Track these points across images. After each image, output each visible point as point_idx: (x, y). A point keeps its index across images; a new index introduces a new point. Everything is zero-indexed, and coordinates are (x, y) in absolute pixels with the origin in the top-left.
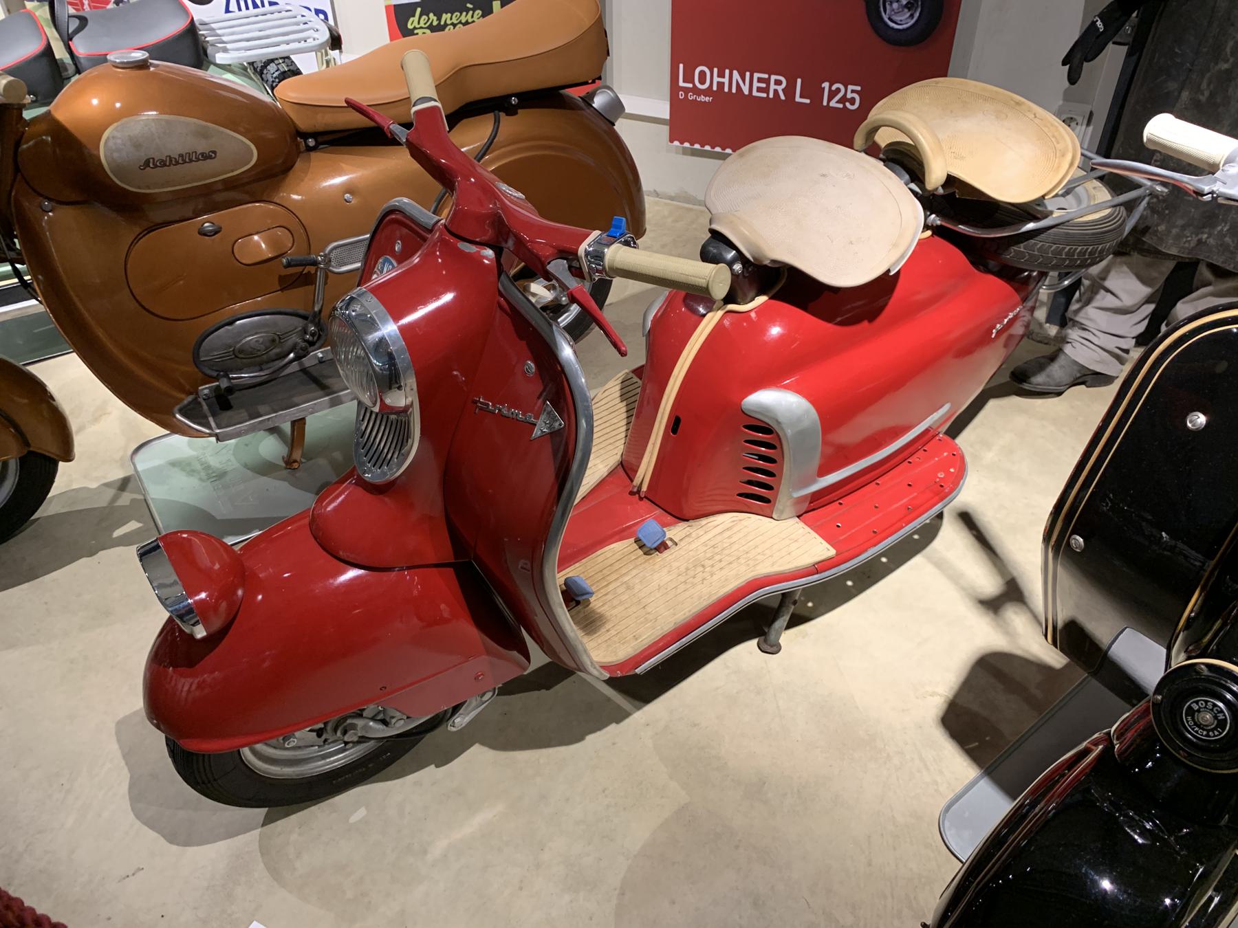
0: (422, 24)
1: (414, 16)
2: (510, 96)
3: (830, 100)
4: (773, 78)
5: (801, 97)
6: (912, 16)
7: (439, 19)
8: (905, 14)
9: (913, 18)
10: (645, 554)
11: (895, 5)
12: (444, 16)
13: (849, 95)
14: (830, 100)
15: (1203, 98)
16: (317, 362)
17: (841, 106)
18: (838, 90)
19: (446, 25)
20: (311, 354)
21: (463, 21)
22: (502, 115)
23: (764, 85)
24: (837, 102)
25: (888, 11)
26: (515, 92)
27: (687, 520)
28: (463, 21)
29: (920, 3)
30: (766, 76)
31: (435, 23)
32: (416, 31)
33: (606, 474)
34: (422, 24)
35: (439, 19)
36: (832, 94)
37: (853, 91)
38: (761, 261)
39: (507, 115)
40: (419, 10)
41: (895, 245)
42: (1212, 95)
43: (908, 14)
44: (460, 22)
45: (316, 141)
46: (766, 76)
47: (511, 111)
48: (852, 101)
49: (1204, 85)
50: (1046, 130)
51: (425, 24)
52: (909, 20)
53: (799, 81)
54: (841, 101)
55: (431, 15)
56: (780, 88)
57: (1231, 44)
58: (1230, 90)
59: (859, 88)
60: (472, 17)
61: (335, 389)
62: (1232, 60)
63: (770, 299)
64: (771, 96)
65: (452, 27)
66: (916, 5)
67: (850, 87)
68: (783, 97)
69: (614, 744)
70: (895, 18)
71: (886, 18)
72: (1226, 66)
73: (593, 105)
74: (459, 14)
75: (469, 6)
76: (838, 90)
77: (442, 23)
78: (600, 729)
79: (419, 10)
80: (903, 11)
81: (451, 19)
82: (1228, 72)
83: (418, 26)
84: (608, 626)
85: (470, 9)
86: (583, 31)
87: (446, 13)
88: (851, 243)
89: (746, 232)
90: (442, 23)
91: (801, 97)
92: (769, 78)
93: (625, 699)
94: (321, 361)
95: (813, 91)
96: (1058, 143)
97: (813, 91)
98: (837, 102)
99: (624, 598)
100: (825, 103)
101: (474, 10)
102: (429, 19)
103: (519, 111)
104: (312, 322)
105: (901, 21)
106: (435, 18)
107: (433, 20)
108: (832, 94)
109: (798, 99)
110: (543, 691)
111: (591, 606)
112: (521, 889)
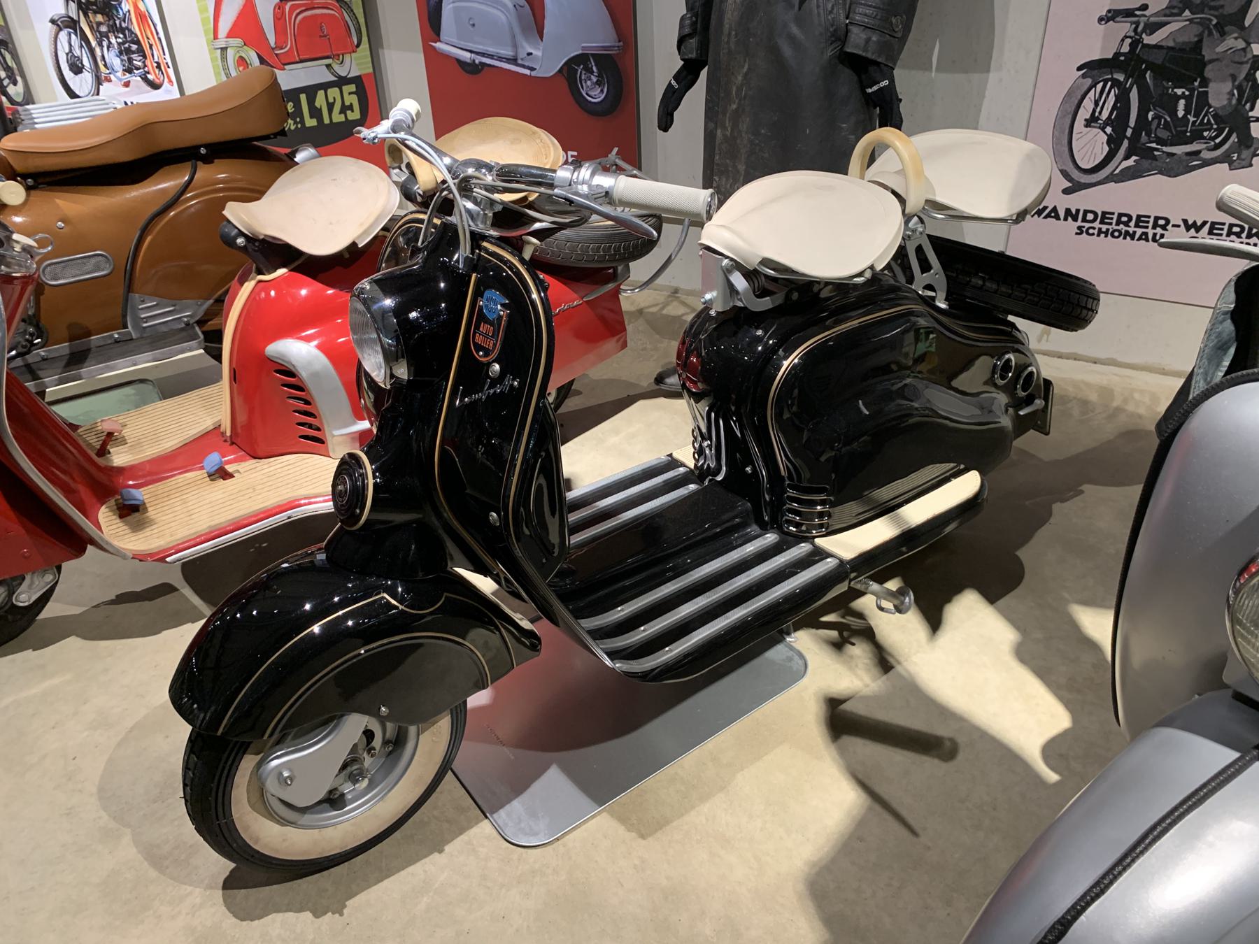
2: (201, 146)
6: (602, 91)
8: (597, 90)
9: (603, 93)
10: (211, 480)
11: (589, 83)
15: (728, 133)
16: (41, 359)
20: (34, 352)
22: (199, 163)
25: (584, 88)
26: (204, 142)
27: (261, 459)
29: (606, 80)
33: (212, 428)
38: (257, 237)
39: (204, 163)
41: (361, 224)
42: (732, 130)
43: (599, 90)
45: (35, 181)
47: (207, 160)
49: (727, 125)
50: (543, 150)
52: (600, 95)
57: (734, 89)
58: (740, 126)
59: (575, 153)
61: (42, 376)
62: (737, 101)
63: (290, 271)
66: (603, 82)
69: (182, 636)
70: (590, 93)
72: (734, 106)
73: (295, 159)
78: (176, 626)
80: (595, 87)
82: (737, 110)
84: (153, 527)
86: (255, 94)
88: (331, 224)
89: (244, 217)
93: (209, 607)
94: (44, 359)
96: (546, 158)
99: (176, 509)
103: (216, 161)
104: (30, 324)
105: (595, 95)
110: (147, 602)
111: (148, 514)
112: (53, 728)
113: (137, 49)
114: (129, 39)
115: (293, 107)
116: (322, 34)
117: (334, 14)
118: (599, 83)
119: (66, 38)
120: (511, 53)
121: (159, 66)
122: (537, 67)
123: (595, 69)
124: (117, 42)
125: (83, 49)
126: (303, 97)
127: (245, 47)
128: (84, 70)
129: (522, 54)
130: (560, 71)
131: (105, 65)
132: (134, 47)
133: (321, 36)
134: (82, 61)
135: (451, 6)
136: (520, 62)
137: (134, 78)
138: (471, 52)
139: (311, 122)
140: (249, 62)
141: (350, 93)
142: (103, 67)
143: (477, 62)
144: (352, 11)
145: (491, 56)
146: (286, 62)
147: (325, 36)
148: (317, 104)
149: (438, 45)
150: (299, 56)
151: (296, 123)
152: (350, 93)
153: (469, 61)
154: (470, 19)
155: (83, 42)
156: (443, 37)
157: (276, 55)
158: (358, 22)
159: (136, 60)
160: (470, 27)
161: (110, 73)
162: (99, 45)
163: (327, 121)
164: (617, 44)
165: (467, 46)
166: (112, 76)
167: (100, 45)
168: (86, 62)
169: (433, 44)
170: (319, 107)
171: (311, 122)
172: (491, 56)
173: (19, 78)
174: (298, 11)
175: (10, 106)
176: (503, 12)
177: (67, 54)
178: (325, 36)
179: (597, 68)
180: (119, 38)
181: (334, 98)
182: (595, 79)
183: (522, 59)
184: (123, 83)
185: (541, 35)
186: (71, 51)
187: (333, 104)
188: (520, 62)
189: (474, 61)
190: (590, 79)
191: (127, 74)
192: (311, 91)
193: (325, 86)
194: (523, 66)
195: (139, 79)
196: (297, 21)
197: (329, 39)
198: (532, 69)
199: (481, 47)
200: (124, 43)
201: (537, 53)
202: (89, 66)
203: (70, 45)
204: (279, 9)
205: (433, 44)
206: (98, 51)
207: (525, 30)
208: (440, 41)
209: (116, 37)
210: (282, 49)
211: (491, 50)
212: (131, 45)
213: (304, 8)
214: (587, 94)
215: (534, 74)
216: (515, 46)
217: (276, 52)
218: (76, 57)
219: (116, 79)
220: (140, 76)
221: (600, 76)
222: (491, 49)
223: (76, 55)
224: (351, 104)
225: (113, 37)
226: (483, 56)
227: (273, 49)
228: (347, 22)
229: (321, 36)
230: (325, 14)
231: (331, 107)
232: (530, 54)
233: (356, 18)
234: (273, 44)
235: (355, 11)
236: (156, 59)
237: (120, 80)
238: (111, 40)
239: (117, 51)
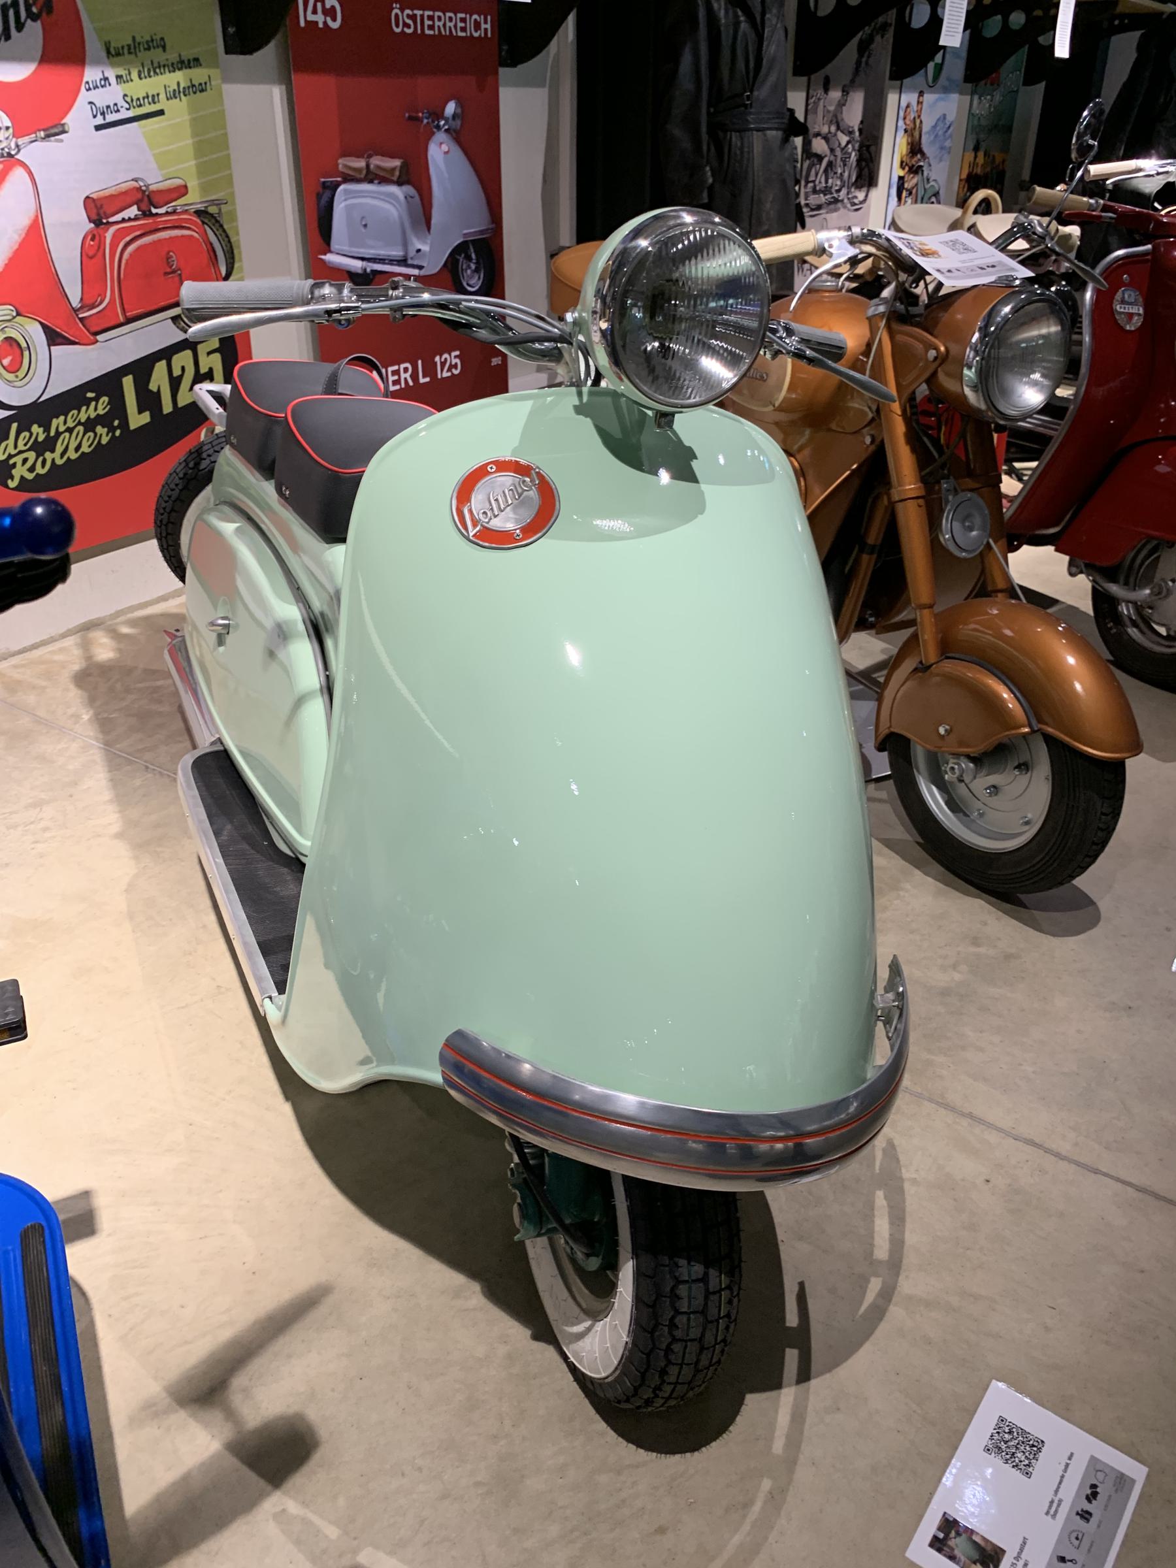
0: (21, 447)
1: (7, 438)
3: (442, 370)
4: (402, 366)
5: (424, 377)
7: (47, 429)
12: (55, 422)
13: (454, 362)
14: (442, 370)
17: (449, 374)
18: (446, 359)
19: (58, 434)
21: (83, 420)
23: (396, 377)
24: (448, 371)
28: (83, 420)
30: (396, 368)
31: (41, 438)
32: (11, 462)
34: (21, 447)
35: (47, 429)
36: (443, 364)
37: (456, 357)
40: (15, 426)
43: (477, 278)
44: (79, 423)
46: (396, 368)
48: (455, 366)
51: (25, 445)
53: (420, 362)
54: (449, 370)
55: (35, 429)
56: (408, 375)
59: (457, 353)
60: (96, 409)
64: (403, 386)
65: (67, 435)
67: (454, 354)
68: (411, 383)
70: (471, 282)
71: (465, 284)
74: (75, 412)
75: (90, 395)
76: (446, 359)
77: (52, 433)
79: (15, 426)
81: (65, 422)
83: (14, 452)
85: (91, 399)
87: (57, 417)
90: (52, 433)
91: (424, 377)
92: (399, 370)
95: (430, 370)
97: (430, 370)
98: (448, 371)
100: (439, 377)
101: (97, 399)
102: (31, 434)
106: (41, 430)
107: (38, 434)
108: (443, 364)
109: (422, 380)
115: (108, 404)
116: (168, 270)
117: (192, 236)
118: (477, 270)
120: (401, 253)
122: (425, 265)
123: (473, 256)
126: (128, 382)
127: (19, 319)
129: (412, 253)
130: (445, 265)
133: (166, 274)
135: (343, 205)
136: (410, 262)
138: (363, 259)
139: (138, 420)
140: (24, 345)
141: (209, 353)
143: (368, 270)
144: (221, 226)
145: (381, 261)
146: (99, 329)
147: (174, 272)
148: (153, 387)
149: (329, 258)
150: (124, 311)
151: (112, 429)
152: (209, 353)
153: (360, 271)
154: (363, 218)
156: (335, 245)
157: (81, 319)
158: (229, 241)
160: (363, 230)
163: (167, 408)
164: (491, 226)
165: (358, 253)
169: (323, 257)
170: (155, 390)
171: (138, 420)
172: (381, 261)
174: (128, 239)
176: (395, 206)
178: (174, 272)
179: (476, 255)
181: (183, 368)
182: (473, 266)
183: (412, 258)
185: (429, 229)
187: (181, 377)
188: (410, 262)
189: (365, 270)
190: (469, 267)
192: (141, 368)
193: (167, 354)
194: (413, 266)
196: (126, 255)
197: (180, 275)
198: (420, 268)
199: (372, 251)
201: (425, 248)
204: (92, 239)
205: (323, 257)
207: (414, 224)
208: (330, 251)
210: (93, 307)
211: (382, 252)
213: (138, 233)
214: (468, 285)
215: (423, 272)
216: (405, 244)
217: (80, 316)
221: (477, 263)
222: (382, 252)
224: (211, 370)
226: (375, 262)
227: (76, 311)
228: (211, 244)
229: (166, 274)
230: (177, 237)
231: (175, 383)
232: (419, 251)
233: (227, 236)
234: (75, 302)
235: (226, 227)
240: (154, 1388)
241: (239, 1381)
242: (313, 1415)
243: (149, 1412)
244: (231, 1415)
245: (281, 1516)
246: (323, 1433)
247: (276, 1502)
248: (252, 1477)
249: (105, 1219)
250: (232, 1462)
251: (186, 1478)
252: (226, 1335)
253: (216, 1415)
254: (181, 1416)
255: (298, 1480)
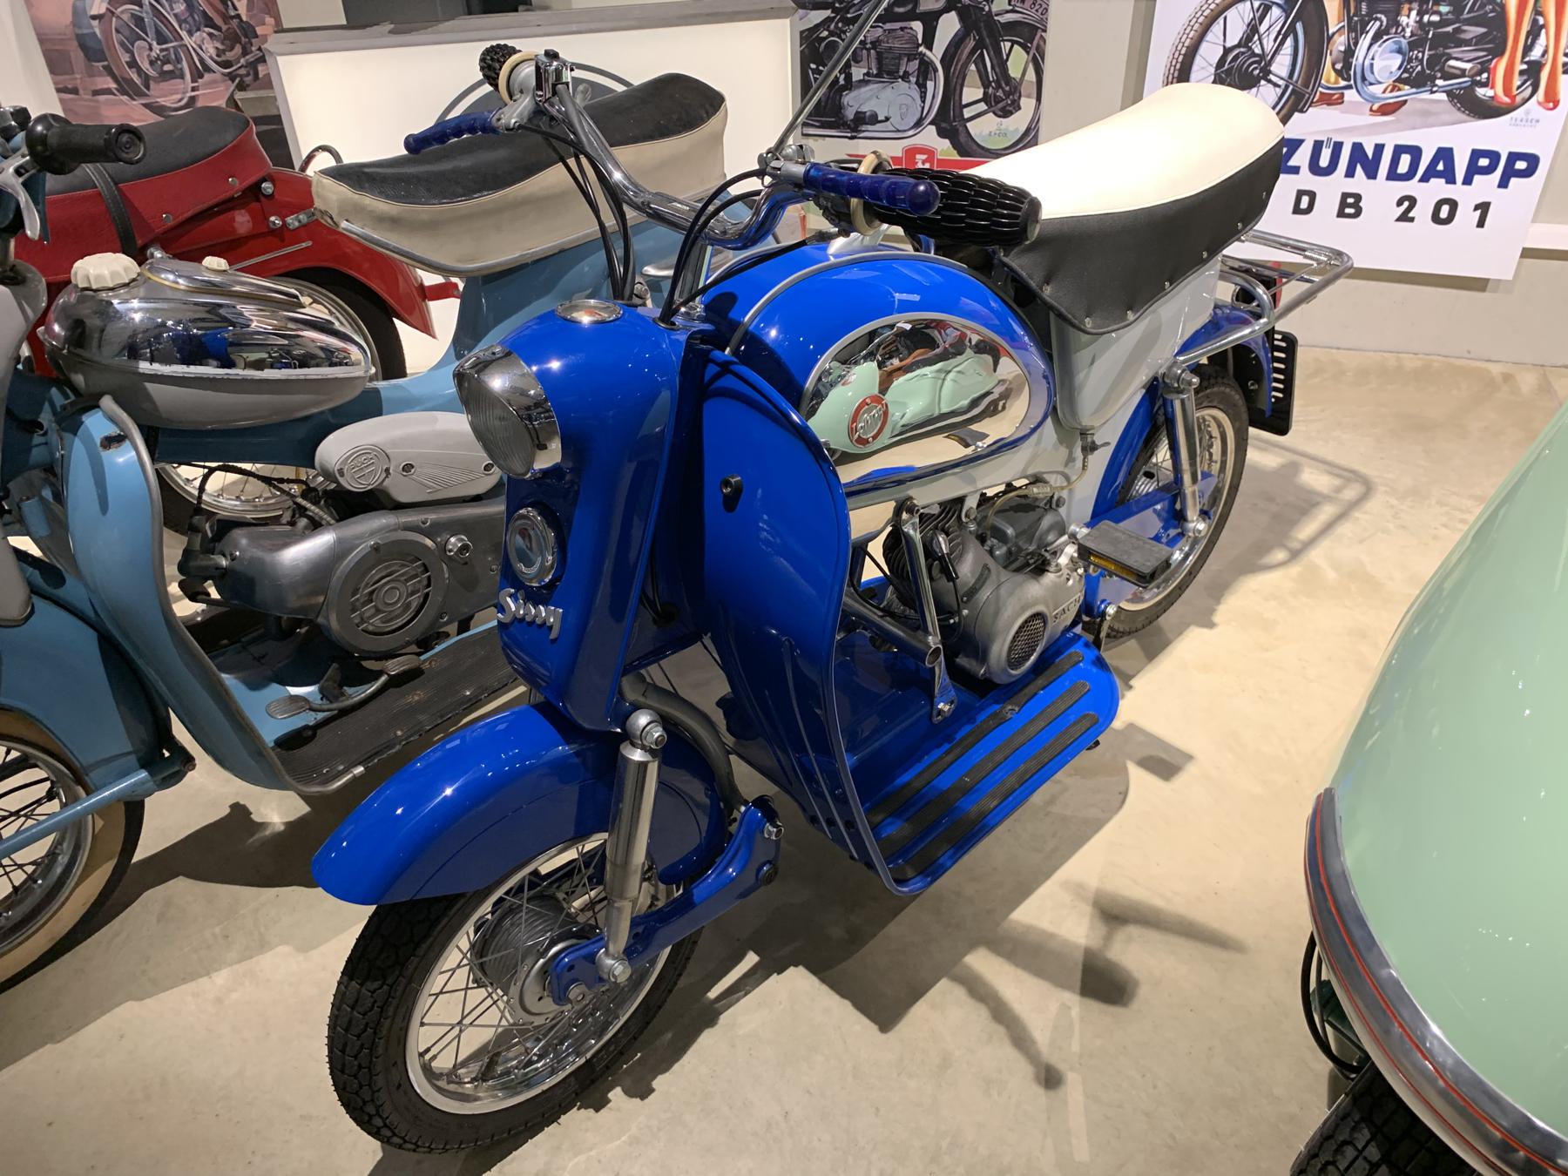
113: (1480, 39)
114: (1465, 16)
119: (1248, 16)
121: (1533, 71)
124: (1420, 22)
125: (1289, 42)
128: (1263, 82)
131: (1344, 73)
132: (1474, 31)
134: (1270, 63)
137: (1426, 96)
142: (1333, 74)
155: (1299, 26)
159: (1457, 59)
161: (1349, 87)
162: (1351, 28)
166: (1350, 95)
167: (1356, 28)
168: (1281, 66)
173: (1028, 104)
175: (959, 158)
177: (1227, 51)
180: (1438, 13)
184: (1375, 107)
186: (1246, 41)
191: (1407, 87)
195: (1444, 96)
200: (1444, 22)
202: (1284, 73)
203: (1253, 30)
206: (1340, 44)
209: (1421, 14)
212: (1465, 28)
218: (1254, 55)
219: (1357, 98)
220: (1449, 93)
223: (1258, 50)
225: (1414, 13)
236: (1536, 54)
237: (1373, 98)
238: (1403, 20)
239: (1404, 42)
240: (1093, 883)
241: (1133, 930)
242: (1143, 992)
243: (1077, 889)
244: (1108, 938)
245: (1065, 1008)
246: (1136, 1005)
247: (1072, 999)
248: (1078, 976)
249: (1180, 780)
250: (1079, 957)
251: (1052, 936)
252: (1159, 902)
253: (1101, 929)
254: (1087, 909)
255: (1095, 1006)
